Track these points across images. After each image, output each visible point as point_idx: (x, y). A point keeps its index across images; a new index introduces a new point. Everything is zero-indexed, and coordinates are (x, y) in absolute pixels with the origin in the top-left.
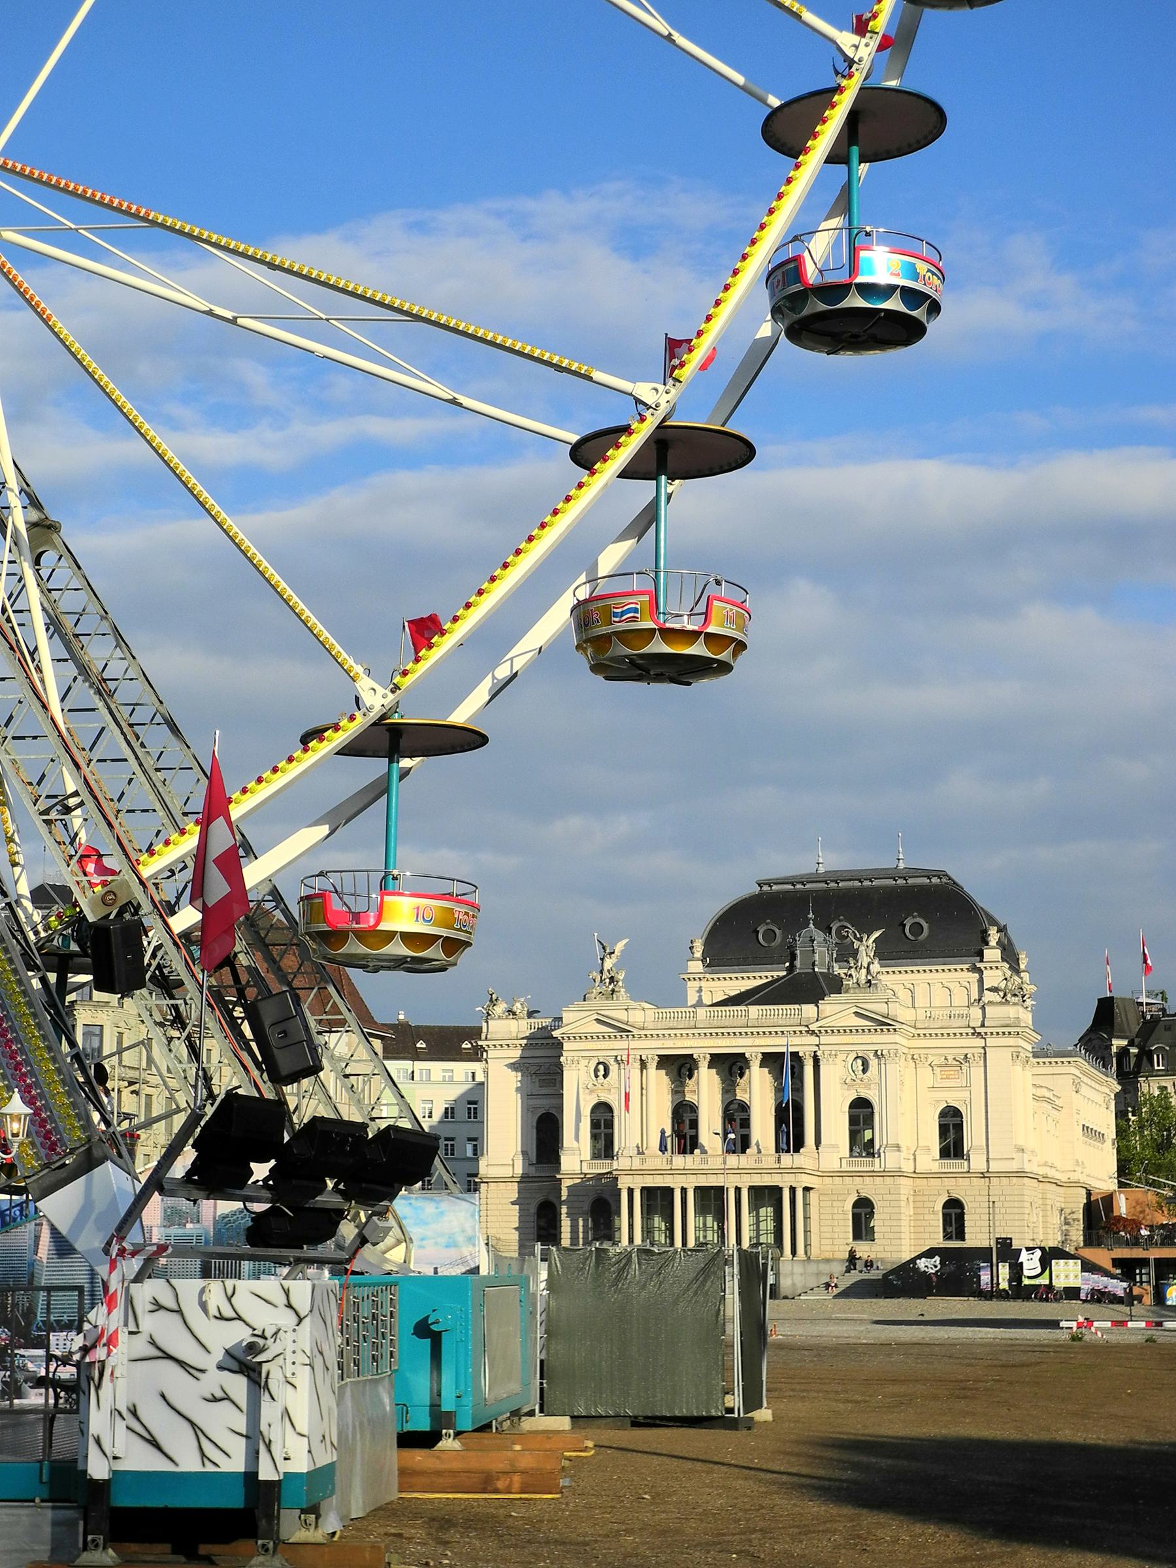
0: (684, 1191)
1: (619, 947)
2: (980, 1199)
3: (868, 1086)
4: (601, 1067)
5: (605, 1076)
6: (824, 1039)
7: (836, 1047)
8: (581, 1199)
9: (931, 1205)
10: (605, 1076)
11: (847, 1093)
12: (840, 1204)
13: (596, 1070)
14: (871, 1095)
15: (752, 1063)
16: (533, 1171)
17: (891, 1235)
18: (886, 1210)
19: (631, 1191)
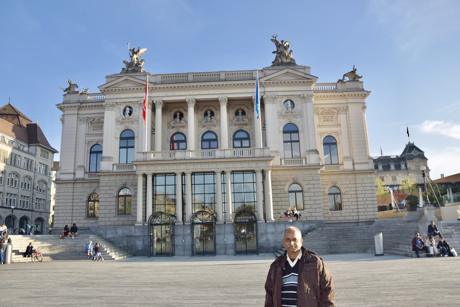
0: (183, 174)
1: (142, 51)
2: (351, 186)
3: (295, 116)
4: (128, 109)
5: (130, 114)
6: (267, 89)
7: (275, 93)
8: (112, 188)
9: (323, 190)
10: (130, 114)
11: (282, 120)
12: (281, 187)
13: (125, 110)
14: (296, 121)
15: (221, 104)
16: (87, 177)
17: (315, 206)
18: (311, 190)
19: (145, 176)
